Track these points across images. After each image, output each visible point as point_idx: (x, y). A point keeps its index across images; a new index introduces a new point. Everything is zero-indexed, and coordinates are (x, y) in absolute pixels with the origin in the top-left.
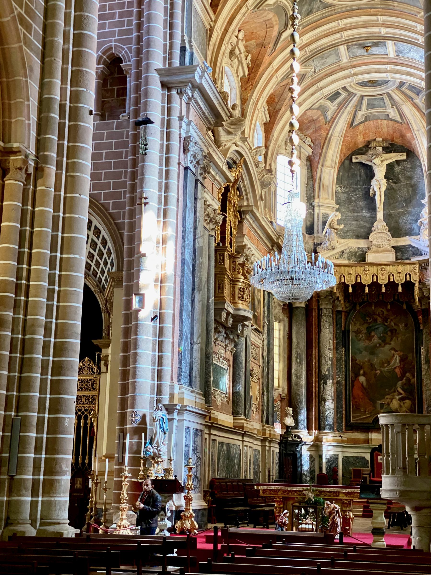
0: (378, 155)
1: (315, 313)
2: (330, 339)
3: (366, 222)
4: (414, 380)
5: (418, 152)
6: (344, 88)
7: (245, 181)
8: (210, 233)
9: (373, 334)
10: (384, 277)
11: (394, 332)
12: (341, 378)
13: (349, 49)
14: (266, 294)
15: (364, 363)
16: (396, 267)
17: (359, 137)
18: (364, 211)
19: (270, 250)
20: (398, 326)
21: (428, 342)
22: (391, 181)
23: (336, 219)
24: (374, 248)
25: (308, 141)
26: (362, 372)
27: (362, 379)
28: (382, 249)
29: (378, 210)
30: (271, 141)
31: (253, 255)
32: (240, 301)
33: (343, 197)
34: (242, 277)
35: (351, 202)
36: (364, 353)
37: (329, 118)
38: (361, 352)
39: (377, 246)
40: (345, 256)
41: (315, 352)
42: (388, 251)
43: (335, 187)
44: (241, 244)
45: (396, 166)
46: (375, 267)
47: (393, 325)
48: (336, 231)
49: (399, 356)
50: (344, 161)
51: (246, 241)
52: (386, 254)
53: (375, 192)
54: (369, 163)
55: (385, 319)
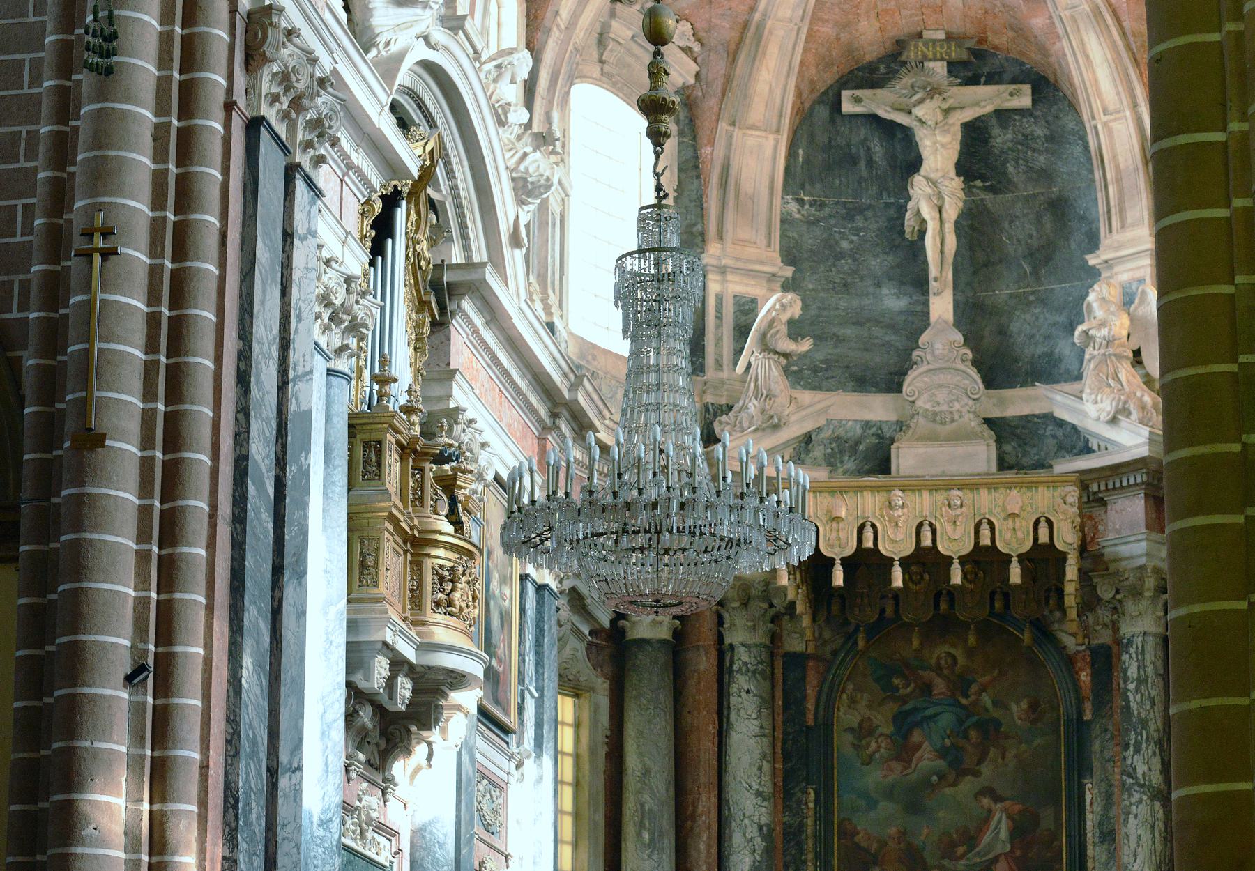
0: (933, 91)
1: (703, 663)
2: (764, 756)
3: (892, 327)
5: (1072, 85)
7: (458, 174)
8: (332, 365)
9: (916, 737)
10: (960, 529)
11: (990, 731)
14: (530, 589)
15: (883, 844)
16: (1000, 495)
17: (864, 24)
18: (885, 291)
19: (545, 428)
20: (1007, 707)
21: (1109, 766)
22: (979, 183)
23: (785, 317)
24: (921, 424)
25: (683, 34)
28: (949, 428)
29: (933, 285)
30: (549, 31)
31: (484, 445)
32: (440, 618)
33: (810, 240)
34: (449, 528)
35: (839, 256)
36: (886, 808)
38: (872, 804)
39: (934, 417)
40: (818, 452)
41: (706, 805)
42: (968, 436)
43: (778, 202)
45: (996, 131)
46: (926, 494)
47: (989, 704)
48: (784, 361)
49: (1009, 817)
50: (812, 109)
51: (460, 396)
52: (962, 449)
53: (923, 222)
55: (961, 684)
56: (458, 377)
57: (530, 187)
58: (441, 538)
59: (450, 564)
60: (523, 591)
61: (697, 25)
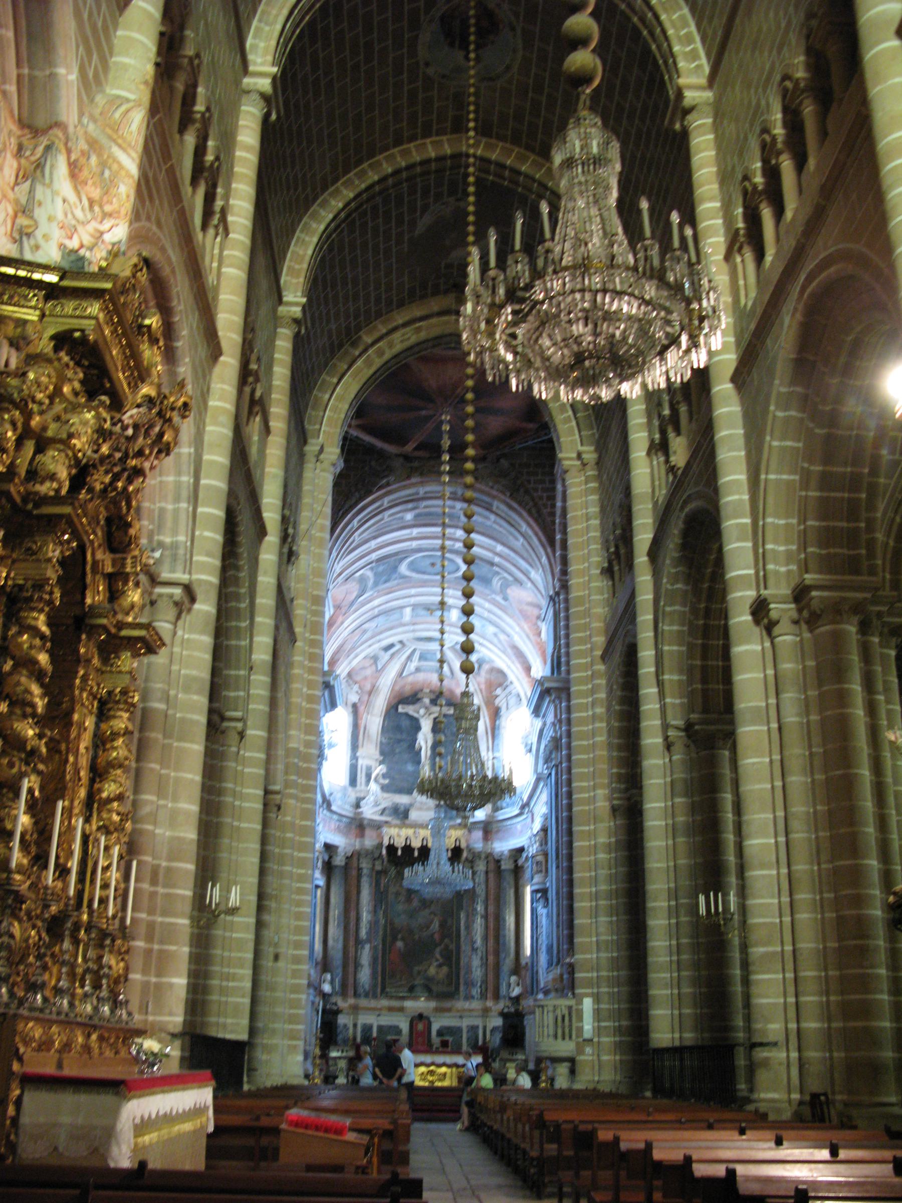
1: (354, 873)
4: (452, 947)
6: (401, 642)
12: (378, 942)
26: (400, 936)
27: (400, 944)
36: (403, 917)
40: (387, 812)
41: (353, 915)
54: (416, 715)
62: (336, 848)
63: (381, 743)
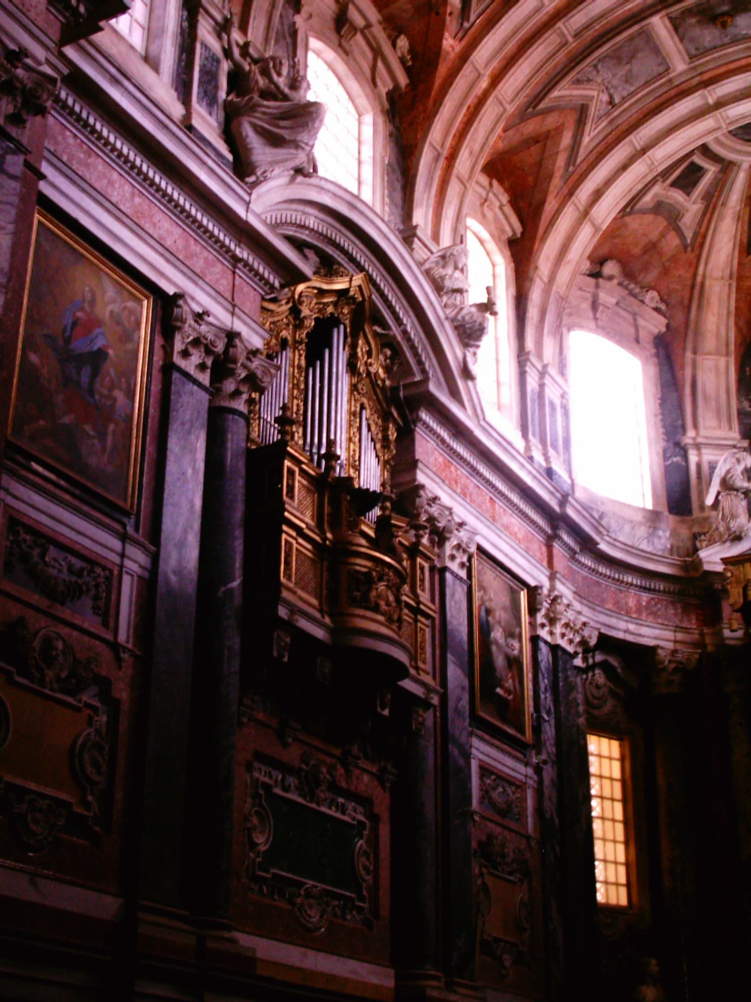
6: (705, 150)
13: (681, 30)
25: (652, 298)
37: (689, 235)
44: (411, 485)
56: (420, 465)
57: (469, 331)
58: (355, 548)
59: (364, 570)
60: (535, 649)
61: (662, 293)
62: (651, 650)
63: (741, 413)
